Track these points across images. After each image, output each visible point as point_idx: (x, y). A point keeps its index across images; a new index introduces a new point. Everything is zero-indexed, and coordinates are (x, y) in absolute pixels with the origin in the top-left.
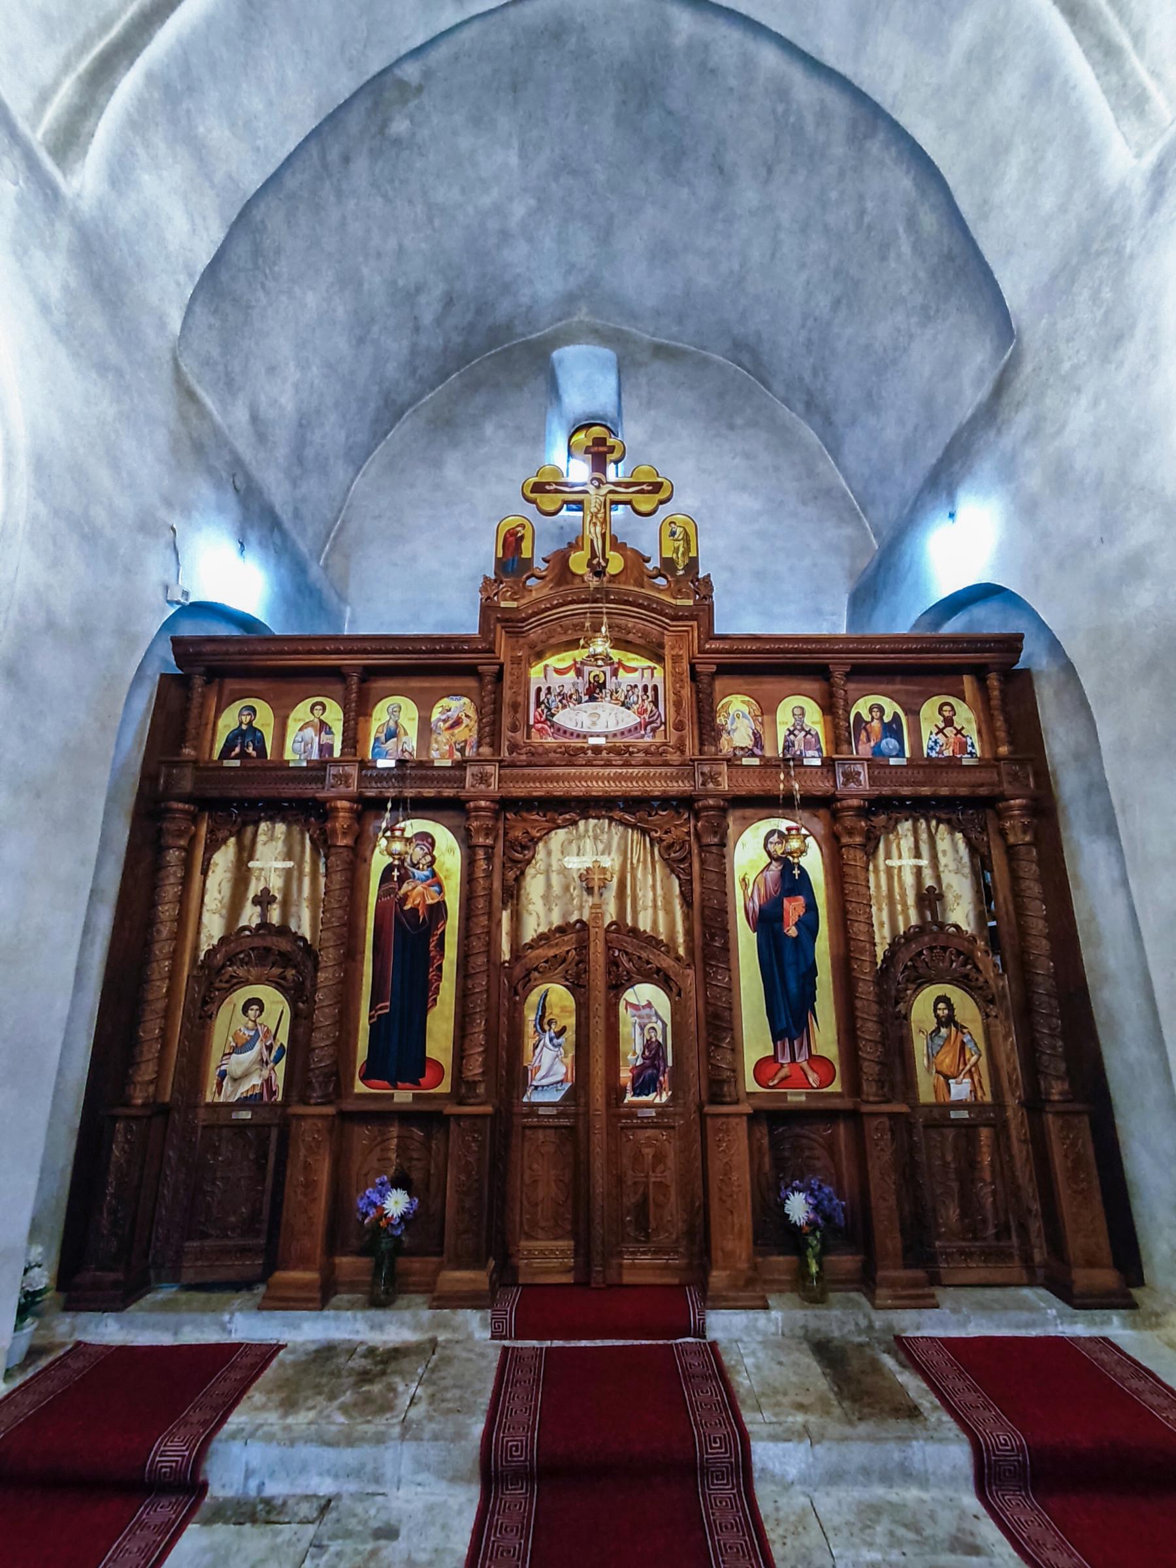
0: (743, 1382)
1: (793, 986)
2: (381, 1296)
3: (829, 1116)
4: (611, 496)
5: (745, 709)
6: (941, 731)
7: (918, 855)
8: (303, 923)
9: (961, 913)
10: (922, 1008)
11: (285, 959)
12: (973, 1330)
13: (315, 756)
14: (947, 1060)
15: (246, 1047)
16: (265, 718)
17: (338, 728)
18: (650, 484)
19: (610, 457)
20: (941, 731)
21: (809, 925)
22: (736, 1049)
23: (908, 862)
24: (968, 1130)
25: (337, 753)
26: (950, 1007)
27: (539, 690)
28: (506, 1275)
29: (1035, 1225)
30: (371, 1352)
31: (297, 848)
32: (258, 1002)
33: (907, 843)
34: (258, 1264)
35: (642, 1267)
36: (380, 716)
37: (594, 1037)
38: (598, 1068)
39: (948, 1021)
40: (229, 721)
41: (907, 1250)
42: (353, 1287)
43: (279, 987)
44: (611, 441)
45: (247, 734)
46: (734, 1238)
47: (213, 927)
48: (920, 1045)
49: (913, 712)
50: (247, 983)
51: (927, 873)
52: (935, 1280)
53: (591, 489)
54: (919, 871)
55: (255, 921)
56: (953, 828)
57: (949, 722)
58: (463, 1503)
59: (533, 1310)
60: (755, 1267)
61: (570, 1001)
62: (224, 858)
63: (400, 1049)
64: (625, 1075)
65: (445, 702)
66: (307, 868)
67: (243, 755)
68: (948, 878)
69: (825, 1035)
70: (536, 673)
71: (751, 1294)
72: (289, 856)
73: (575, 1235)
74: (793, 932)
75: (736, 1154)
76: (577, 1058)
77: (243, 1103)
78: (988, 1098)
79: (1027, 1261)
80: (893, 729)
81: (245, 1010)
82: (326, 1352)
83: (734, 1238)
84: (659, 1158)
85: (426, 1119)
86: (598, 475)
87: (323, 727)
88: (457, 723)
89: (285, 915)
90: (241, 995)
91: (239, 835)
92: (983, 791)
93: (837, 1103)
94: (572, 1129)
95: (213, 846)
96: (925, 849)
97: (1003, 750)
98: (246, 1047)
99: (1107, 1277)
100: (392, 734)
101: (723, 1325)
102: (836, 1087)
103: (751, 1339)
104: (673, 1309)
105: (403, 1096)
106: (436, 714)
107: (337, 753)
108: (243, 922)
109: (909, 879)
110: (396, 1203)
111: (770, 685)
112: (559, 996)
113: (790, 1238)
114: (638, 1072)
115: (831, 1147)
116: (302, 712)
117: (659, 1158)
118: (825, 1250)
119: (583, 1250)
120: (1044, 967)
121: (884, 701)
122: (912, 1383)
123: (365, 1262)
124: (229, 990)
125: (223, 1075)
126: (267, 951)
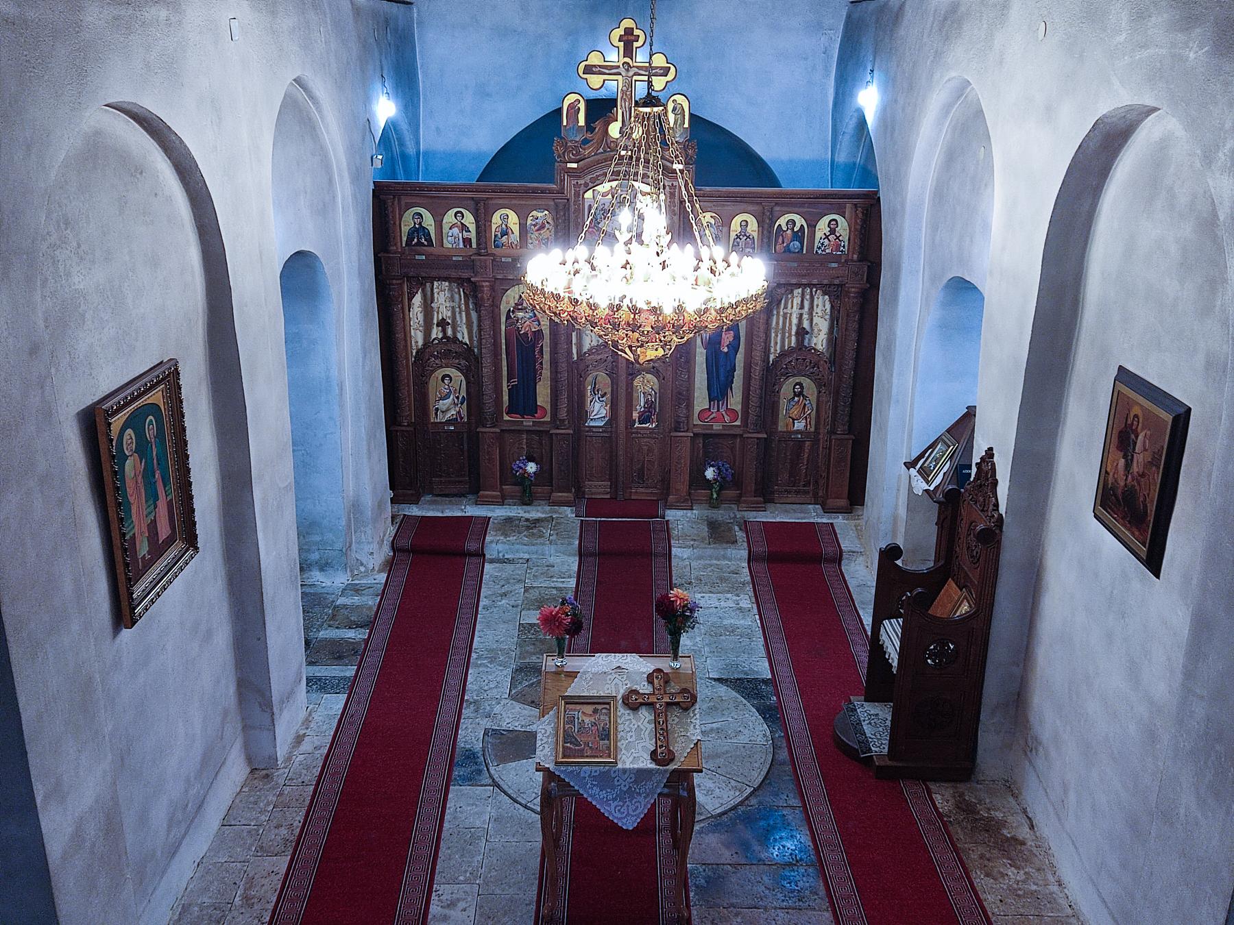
0: (674, 533)
1: (722, 378)
2: (527, 499)
3: (734, 436)
4: (635, 78)
5: (713, 221)
6: (827, 237)
7: (802, 307)
8: (463, 335)
9: (819, 341)
10: (787, 389)
11: (458, 355)
12: (778, 520)
13: (461, 246)
14: (795, 412)
15: (447, 401)
16: (429, 221)
17: (472, 228)
18: (661, 68)
19: (636, 45)
20: (827, 237)
21: (734, 347)
22: (690, 406)
23: (795, 311)
24: (800, 444)
25: (474, 245)
26: (802, 387)
27: (590, 207)
28: (580, 494)
29: (822, 482)
30: (527, 520)
31: (457, 296)
32: (448, 376)
33: (797, 301)
34: (474, 489)
35: (640, 493)
36: (496, 219)
37: (620, 399)
38: (622, 412)
39: (800, 394)
40: (407, 223)
41: (756, 490)
42: (512, 497)
43: (458, 369)
44: (636, 32)
45: (419, 230)
46: (681, 484)
47: (418, 338)
48: (783, 403)
49: (812, 226)
50: (442, 367)
51: (805, 316)
52: (772, 501)
53: (622, 70)
54: (800, 317)
55: (440, 336)
56: (825, 293)
57: (833, 232)
58: (573, 564)
59: (594, 507)
60: (690, 494)
61: (608, 380)
62: (417, 299)
63: (523, 400)
64: (635, 415)
65: (534, 213)
66: (463, 307)
67: (419, 244)
68: (816, 320)
69: (735, 400)
70: (589, 195)
71: (687, 503)
72: (452, 299)
73: (610, 480)
74: (726, 350)
75: (683, 453)
76: (611, 407)
77: (449, 422)
78: (813, 429)
79: (815, 496)
80: (799, 236)
81: (443, 380)
82: (509, 520)
83: (681, 484)
84: (650, 450)
85: (540, 433)
86: (627, 60)
87: (464, 228)
88: (542, 227)
89: (454, 331)
90: (440, 373)
91: (422, 285)
92: (837, 282)
93: (738, 431)
94: (610, 437)
95: (410, 299)
96: (806, 304)
97: (855, 256)
98: (447, 401)
99: (843, 502)
100: (505, 233)
101: (671, 515)
102: (738, 423)
103: (681, 519)
104: (651, 509)
105: (528, 422)
106: (529, 222)
107: (474, 245)
108: (434, 336)
109: (795, 321)
110: (531, 468)
111: (730, 208)
112: (603, 379)
113: (708, 484)
114: (641, 414)
115: (732, 449)
116: (449, 218)
117: (650, 450)
118: (722, 488)
119: (614, 485)
120: (848, 373)
121: (796, 217)
122: (740, 535)
123: (517, 488)
124: (433, 372)
125: (437, 409)
126: (450, 350)
